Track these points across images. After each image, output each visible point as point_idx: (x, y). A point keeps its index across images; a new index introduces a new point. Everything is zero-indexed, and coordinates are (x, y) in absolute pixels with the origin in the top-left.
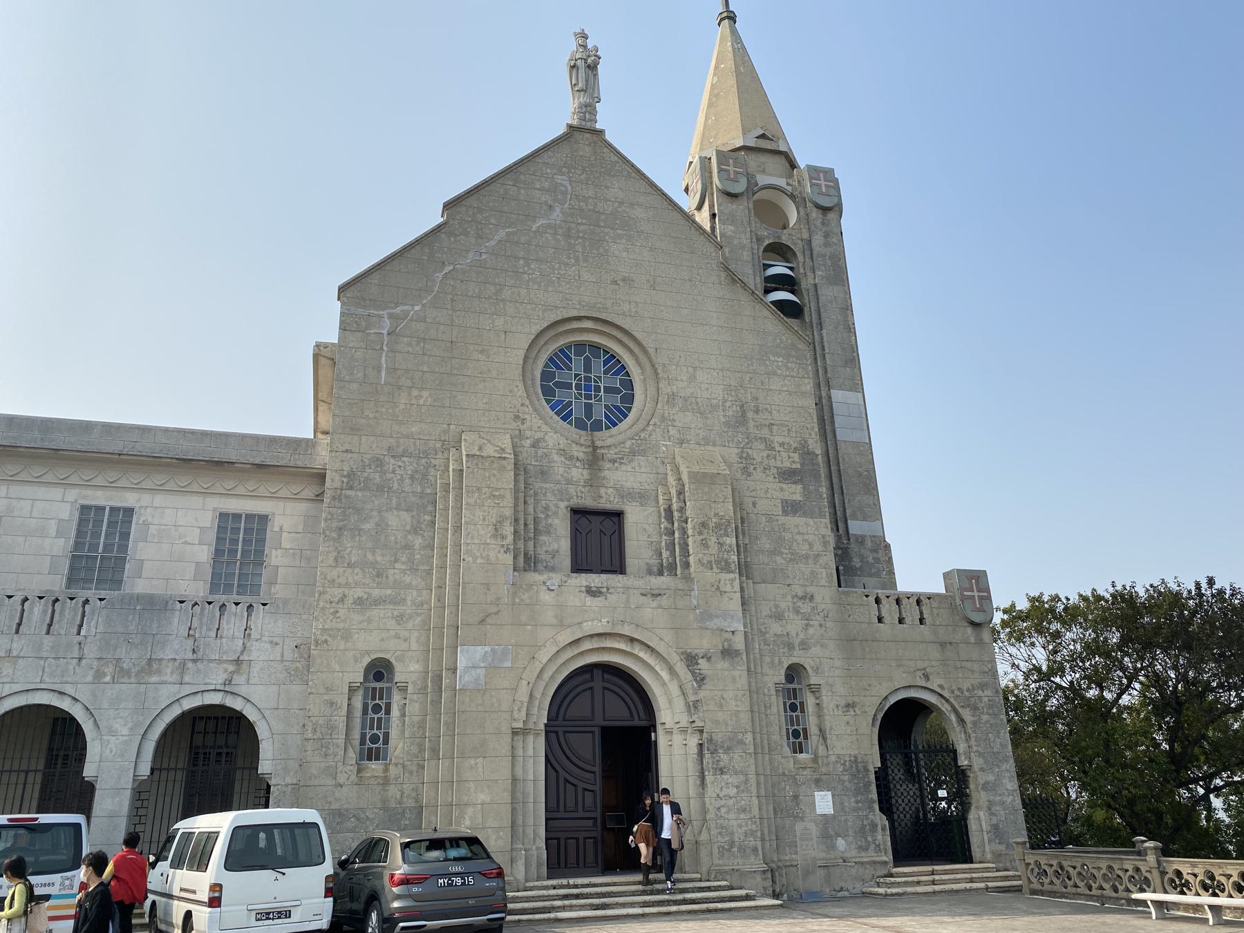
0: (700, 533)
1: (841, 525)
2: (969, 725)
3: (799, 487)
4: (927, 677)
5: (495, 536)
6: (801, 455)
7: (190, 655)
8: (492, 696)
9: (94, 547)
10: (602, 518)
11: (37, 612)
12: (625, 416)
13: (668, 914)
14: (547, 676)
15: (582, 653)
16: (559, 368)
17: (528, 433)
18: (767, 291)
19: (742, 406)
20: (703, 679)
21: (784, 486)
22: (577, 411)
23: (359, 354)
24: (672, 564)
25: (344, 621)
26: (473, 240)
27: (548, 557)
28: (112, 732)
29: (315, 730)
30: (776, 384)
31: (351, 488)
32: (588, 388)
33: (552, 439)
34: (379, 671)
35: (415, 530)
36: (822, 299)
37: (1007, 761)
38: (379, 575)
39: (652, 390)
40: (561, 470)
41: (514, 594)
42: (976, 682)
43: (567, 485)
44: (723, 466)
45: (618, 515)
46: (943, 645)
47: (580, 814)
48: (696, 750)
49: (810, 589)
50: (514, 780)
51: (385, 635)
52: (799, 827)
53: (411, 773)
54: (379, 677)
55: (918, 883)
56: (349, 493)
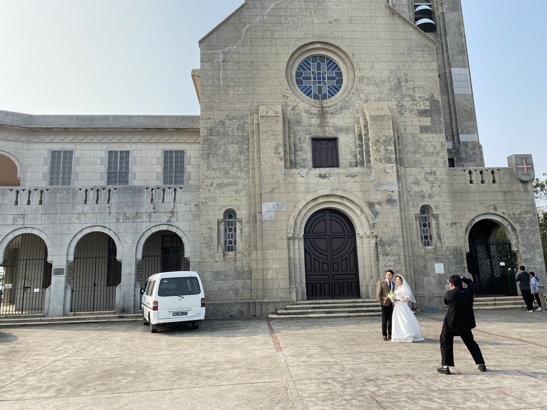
0: (376, 145)
1: (455, 137)
2: (518, 232)
4: (496, 209)
5: (275, 153)
6: (431, 103)
7: (152, 210)
8: (278, 223)
9: (116, 168)
10: (326, 142)
11: (92, 195)
13: (360, 316)
14: (303, 214)
15: (319, 204)
16: (304, 69)
17: (290, 104)
18: (416, 20)
19: (399, 80)
20: (377, 213)
21: (421, 119)
23: (210, 73)
24: (362, 160)
25: (213, 193)
26: (259, 10)
27: (302, 162)
28: (125, 242)
29: (204, 239)
30: (417, 66)
31: (211, 135)
32: (319, 78)
33: (302, 106)
34: (230, 214)
35: (241, 153)
36: (446, 20)
37: (539, 249)
38: (226, 173)
39: (351, 76)
40: (306, 120)
41: (285, 179)
42: (523, 210)
43: (310, 126)
44: (388, 111)
45: (334, 140)
46: (505, 193)
47: (322, 273)
48: (374, 245)
49: (434, 169)
50: (290, 259)
51: (231, 199)
52: (426, 279)
53: (246, 256)
54: (230, 217)
55: (487, 305)
56: (210, 137)
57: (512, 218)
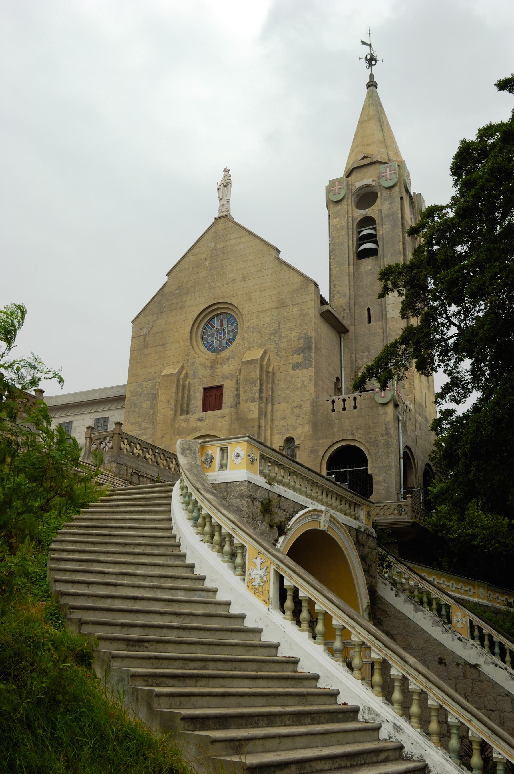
3: (301, 355)
4: (352, 434)
12: (234, 340)
19: (279, 323)
22: (216, 345)
38: (140, 426)
49: (300, 403)
56: (132, 398)
57: (368, 442)
